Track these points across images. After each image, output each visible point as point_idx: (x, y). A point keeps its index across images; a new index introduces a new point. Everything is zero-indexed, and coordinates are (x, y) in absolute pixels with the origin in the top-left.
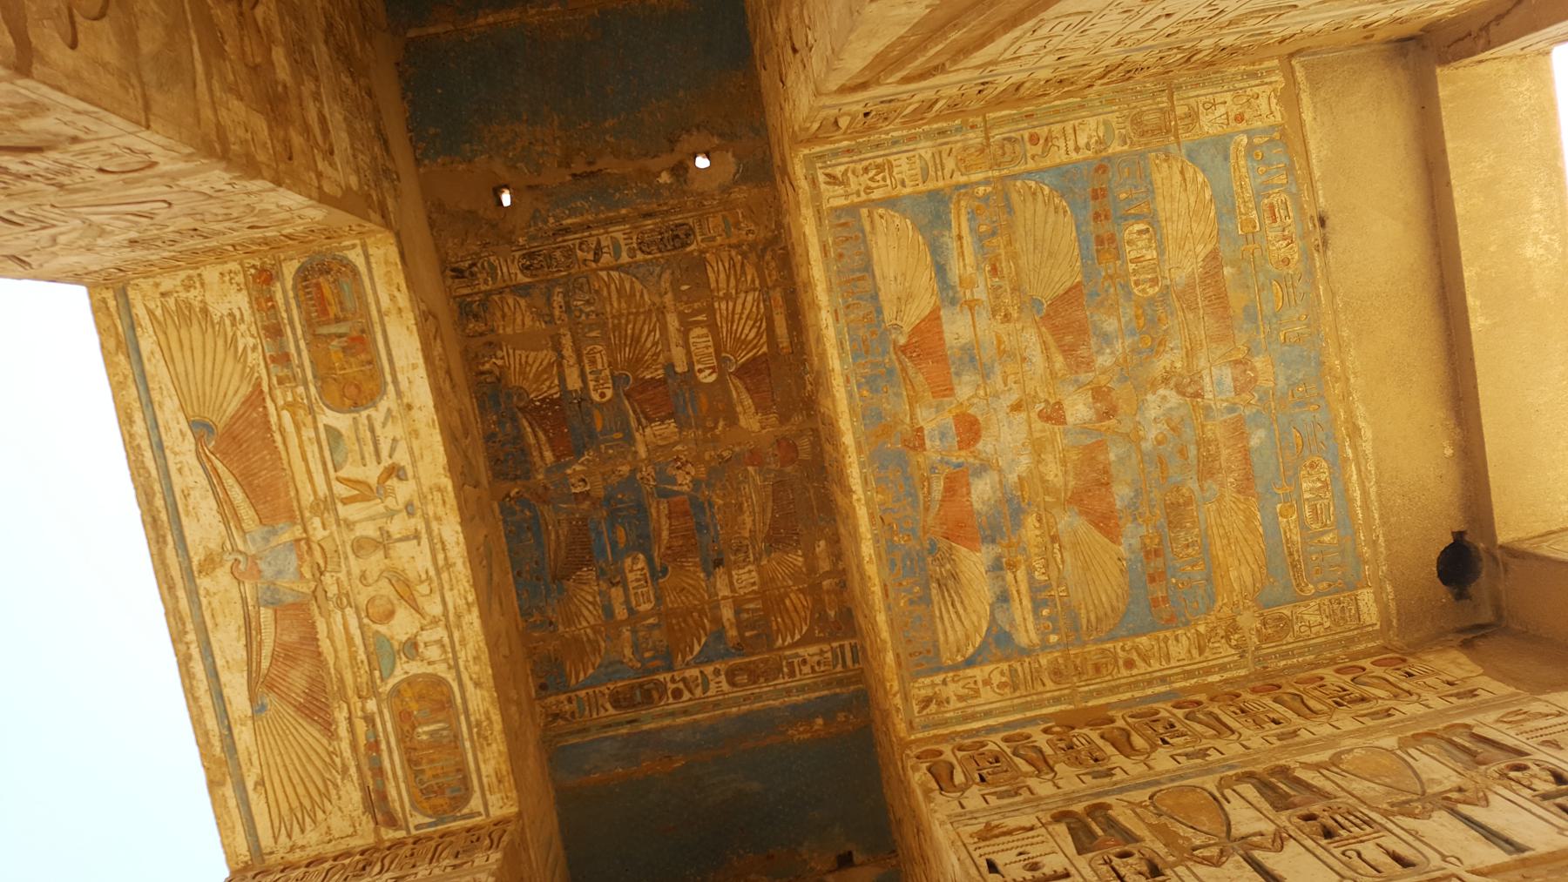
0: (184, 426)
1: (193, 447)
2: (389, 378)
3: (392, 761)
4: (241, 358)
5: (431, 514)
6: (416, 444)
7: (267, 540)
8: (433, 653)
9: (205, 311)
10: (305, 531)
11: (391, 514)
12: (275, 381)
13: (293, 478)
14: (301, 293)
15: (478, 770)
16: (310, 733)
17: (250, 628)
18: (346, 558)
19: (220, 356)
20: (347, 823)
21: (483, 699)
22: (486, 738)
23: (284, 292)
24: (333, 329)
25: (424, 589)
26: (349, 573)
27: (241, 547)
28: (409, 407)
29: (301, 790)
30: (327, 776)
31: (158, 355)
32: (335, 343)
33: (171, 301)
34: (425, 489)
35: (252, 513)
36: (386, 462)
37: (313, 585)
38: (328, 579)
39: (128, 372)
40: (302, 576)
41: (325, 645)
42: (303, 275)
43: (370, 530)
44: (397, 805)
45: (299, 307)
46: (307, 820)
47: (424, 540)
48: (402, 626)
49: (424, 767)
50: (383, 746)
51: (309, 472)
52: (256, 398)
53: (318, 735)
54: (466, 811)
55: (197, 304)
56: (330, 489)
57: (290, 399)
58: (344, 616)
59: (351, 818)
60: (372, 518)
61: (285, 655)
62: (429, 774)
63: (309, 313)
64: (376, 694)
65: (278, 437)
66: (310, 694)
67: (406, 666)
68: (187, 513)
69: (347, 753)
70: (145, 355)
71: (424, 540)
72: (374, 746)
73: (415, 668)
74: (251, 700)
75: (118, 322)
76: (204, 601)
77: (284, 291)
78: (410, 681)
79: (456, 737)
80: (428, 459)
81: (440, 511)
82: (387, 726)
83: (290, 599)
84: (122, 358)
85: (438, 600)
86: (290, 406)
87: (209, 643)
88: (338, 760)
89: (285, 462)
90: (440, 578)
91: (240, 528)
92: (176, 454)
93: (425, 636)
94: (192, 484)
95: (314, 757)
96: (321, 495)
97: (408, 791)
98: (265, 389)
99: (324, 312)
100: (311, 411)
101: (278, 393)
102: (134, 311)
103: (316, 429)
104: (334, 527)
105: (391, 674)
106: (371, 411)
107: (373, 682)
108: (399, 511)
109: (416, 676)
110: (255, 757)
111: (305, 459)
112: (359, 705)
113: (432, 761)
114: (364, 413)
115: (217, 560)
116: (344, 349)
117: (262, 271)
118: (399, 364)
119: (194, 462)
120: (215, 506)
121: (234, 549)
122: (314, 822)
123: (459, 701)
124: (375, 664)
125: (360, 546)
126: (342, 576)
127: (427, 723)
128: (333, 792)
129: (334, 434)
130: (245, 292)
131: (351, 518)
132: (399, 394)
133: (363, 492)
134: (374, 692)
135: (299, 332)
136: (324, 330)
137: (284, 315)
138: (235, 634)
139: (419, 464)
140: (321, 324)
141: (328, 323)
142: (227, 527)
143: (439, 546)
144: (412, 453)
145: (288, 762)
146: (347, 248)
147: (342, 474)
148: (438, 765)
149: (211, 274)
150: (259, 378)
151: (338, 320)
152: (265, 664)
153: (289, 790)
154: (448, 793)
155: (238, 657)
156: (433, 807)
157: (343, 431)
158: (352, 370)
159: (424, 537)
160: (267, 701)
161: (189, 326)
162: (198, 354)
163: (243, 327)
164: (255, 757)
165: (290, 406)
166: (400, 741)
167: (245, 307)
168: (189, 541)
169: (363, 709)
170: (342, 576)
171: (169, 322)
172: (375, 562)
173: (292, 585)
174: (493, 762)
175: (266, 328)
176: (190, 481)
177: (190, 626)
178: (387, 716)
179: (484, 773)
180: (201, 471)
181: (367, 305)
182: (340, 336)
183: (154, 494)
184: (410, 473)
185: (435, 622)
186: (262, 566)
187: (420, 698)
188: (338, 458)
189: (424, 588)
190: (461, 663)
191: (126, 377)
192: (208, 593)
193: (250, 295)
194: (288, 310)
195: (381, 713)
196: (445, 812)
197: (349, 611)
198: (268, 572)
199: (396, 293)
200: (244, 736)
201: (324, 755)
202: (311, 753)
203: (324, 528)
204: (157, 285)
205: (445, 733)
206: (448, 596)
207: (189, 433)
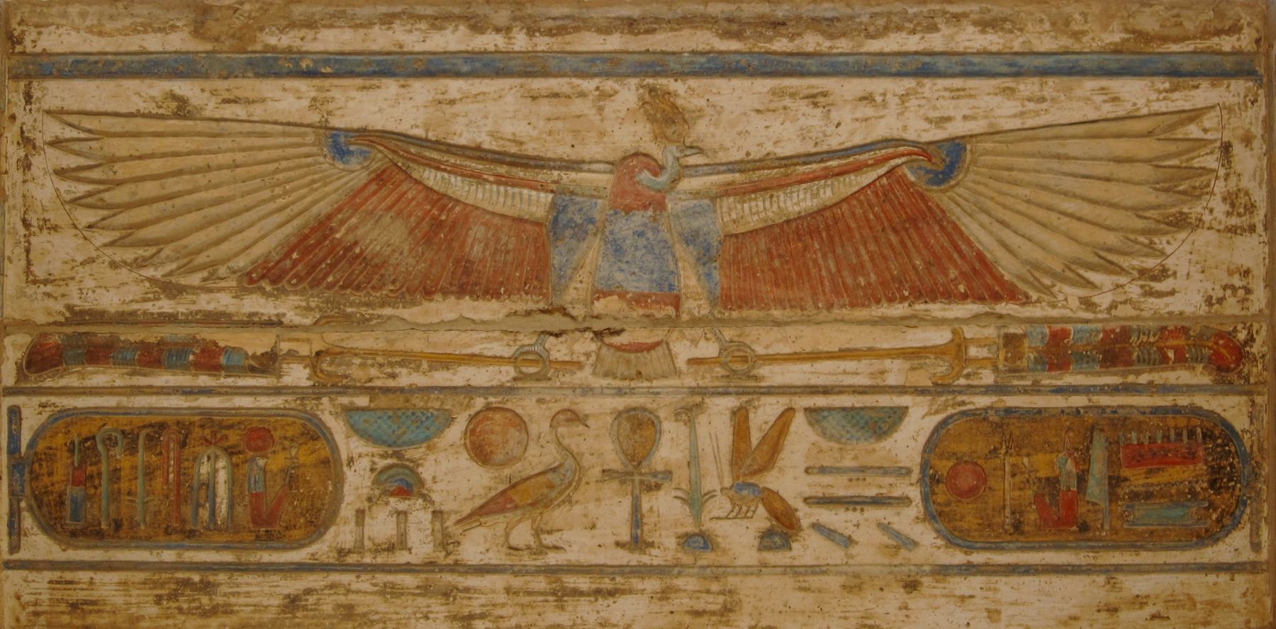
0: (957, 128)
1: (911, 135)
2: (978, 558)
3: (168, 393)
4: (1072, 272)
5: (680, 582)
6: (833, 582)
7: (691, 238)
8: (381, 526)
9: (1180, 222)
10: (695, 322)
11: (695, 500)
12: (1014, 329)
13: (808, 321)
14: (1182, 422)
15: (110, 566)
16: (267, 237)
17: (513, 164)
18: (620, 392)
19: (1084, 232)
20: (57, 269)
21: (258, 608)
22: (173, 596)
23: (1190, 389)
24: (1098, 468)
25: (522, 535)
26: (587, 390)
27: (687, 184)
28: (912, 586)
29: (149, 189)
30: (167, 251)
31: (1108, 110)
32: (1070, 465)
33: (1211, 162)
34: (732, 581)
35: (753, 222)
36: (806, 515)
37: (578, 311)
38: (585, 345)
39: (1087, 43)
40: (599, 294)
41: (445, 308)
42: (1218, 434)
43: (670, 449)
44: (71, 381)
45: (1155, 410)
46: (82, 189)
47: (624, 557)
48: (453, 474)
49: (141, 457)
50: (204, 380)
51: (815, 356)
52: (985, 283)
53: (258, 251)
54: (28, 521)
55: (1195, 209)
56: (771, 391)
57: (973, 351)
58: (498, 360)
59: (66, 280)
60: (693, 461)
61: (440, 222)
62: (125, 462)
63: (1139, 426)
64: (318, 391)
65: (899, 310)
66: (348, 255)
67: (364, 463)
68: (777, 93)
69: (205, 303)
70: (1115, 84)
71: (624, 557)
72: (210, 359)
73: (357, 481)
74: (363, 134)
75: (1188, 47)
76: (589, 85)
77: (1189, 386)
78: (331, 466)
79: (191, 534)
80: (796, 599)
81: (681, 602)
82: (246, 398)
83: (556, 260)
84: (1115, 37)
85: (494, 558)
86: (958, 347)
87: (500, 73)
88: (195, 279)
89: (846, 312)
90: (538, 571)
91: (728, 191)
92: (904, 98)
93: (420, 517)
94: (835, 116)
95: (213, 233)
96: (764, 371)
97: (96, 411)
98: (1003, 308)
99: (1138, 457)
100: (939, 388)
101: (990, 332)
102: (1205, 84)
103: (901, 390)
104: (689, 382)
105: (356, 430)
106: (916, 509)
107: (345, 390)
108: (697, 516)
109: (339, 481)
110: (240, 111)
111: (844, 354)
112: (304, 350)
113: (149, 473)
114: (915, 493)
115: (669, 132)
116: (1052, 482)
117: (1240, 353)
118: (1006, 587)
119: (881, 130)
120: (781, 152)
121: (685, 170)
122: (75, 201)
123: (267, 557)
124: (383, 401)
125: (639, 426)
126: (584, 376)
127: (233, 482)
128: (129, 255)
129: (882, 423)
130: (1204, 310)
131: (702, 419)
132: (943, 571)
133: (753, 456)
134: (325, 386)
135: (1105, 400)
136: (1098, 452)
137: (1144, 379)
138: (508, 129)
139: (789, 581)
140: (1112, 444)
141: (1111, 462)
142: (732, 167)
143: (607, 584)
144: (817, 570)
145: (214, 176)
146: (1255, 532)
147: (799, 423)
148: (139, 486)
149: (1251, 252)
150: (1027, 301)
151: (1115, 482)
152: (431, 178)
153: (155, 166)
154: (72, 491)
155: (459, 125)
156: (49, 455)
157: (887, 443)
158: (1006, 490)
159: (633, 559)
160: (354, 163)
161: (1155, 185)
162: (1096, 190)
163: (1134, 291)
164: (240, 111)
165: (958, 347)
166: (207, 413)
167: (1175, 305)
168: (720, 83)
169: (292, 355)
170: (584, 376)
171: (1172, 148)
172: (600, 447)
173: (584, 266)
174: (119, 600)
175: (1125, 333)
176: (844, 114)
177: (542, 43)
178: (266, 402)
179: (99, 577)
180: (858, 140)
181: (1135, 547)
182: (1082, 479)
183: (831, 37)
184: (771, 557)
185: (446, 542)
186: (639, 218)
187: (291, 478)
188: (832, 423)
189: (522, 535)
190: (346, 578)
191: (1077, 35)
192: (604, 95)
193: (1196, 318)
194: (1151, 388)
195: (277, 391)
196: (35, 477)
197: (506, 374)
198: (625, 227)
199: (1150, 610)
200: (288, 99)
201: (214, 253)
202: (223, 229)
203: (693, 362)
204: (1247, 140)
205: (204, 514)
206: (498, 581)
207: (940, 135)
